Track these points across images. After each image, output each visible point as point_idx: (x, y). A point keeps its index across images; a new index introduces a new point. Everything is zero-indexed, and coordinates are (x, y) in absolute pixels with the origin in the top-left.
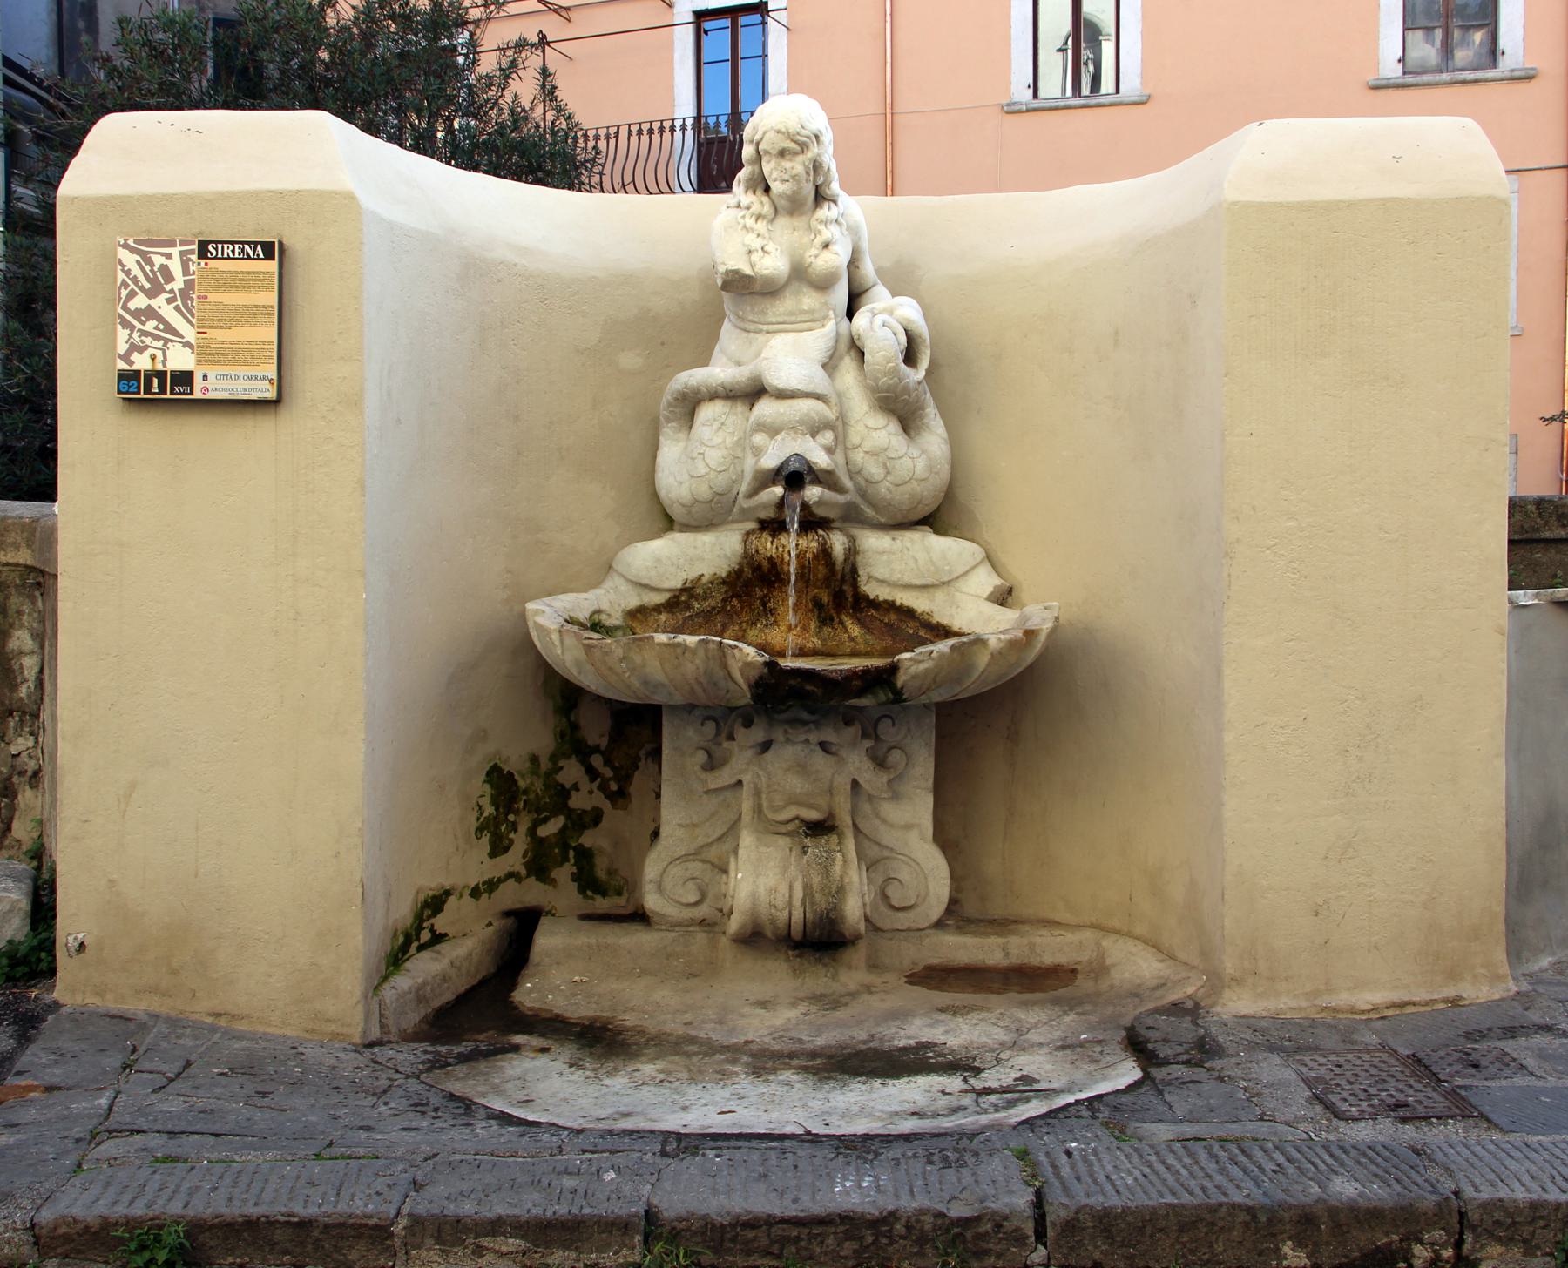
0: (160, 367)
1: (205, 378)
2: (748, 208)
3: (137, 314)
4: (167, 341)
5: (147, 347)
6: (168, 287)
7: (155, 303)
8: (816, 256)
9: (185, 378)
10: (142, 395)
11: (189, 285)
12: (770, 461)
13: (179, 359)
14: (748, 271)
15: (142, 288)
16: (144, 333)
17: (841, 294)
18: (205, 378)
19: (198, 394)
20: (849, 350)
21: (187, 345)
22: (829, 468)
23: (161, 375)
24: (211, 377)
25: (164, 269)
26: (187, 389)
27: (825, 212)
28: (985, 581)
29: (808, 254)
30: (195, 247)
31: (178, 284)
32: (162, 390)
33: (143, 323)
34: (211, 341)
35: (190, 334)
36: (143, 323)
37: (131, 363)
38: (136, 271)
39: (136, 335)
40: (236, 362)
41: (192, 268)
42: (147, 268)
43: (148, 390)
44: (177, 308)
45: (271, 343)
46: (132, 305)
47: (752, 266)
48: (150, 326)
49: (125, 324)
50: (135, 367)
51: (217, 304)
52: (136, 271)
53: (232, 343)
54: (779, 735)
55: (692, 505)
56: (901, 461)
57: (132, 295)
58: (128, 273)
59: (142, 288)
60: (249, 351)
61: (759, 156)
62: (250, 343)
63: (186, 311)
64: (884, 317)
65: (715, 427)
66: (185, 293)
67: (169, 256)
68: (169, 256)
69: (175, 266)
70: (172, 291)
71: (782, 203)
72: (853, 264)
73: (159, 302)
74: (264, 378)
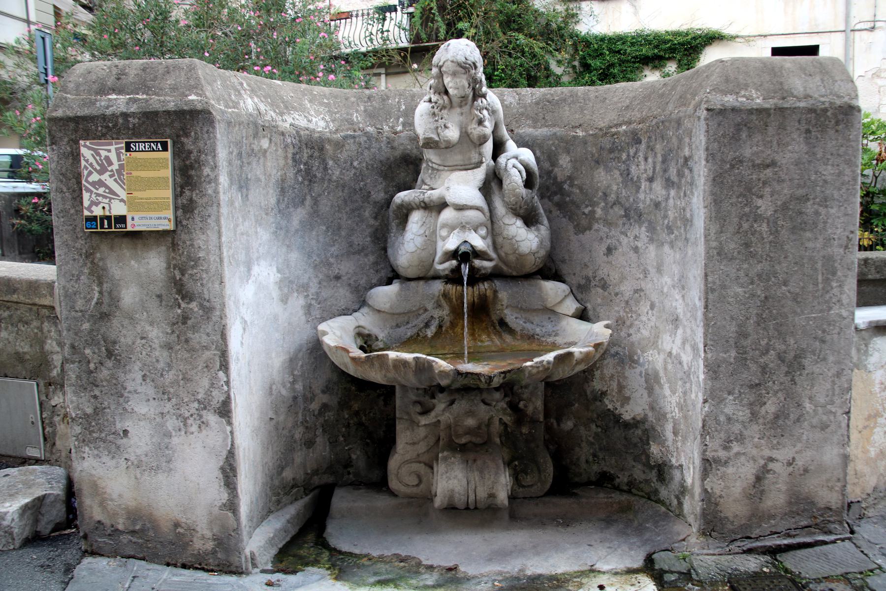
0: (108, 214)
1: (133, 219)
2: (436, 103)
3: (93, 184)
4: (111, 199)
5: (100, 203)
6: (110, 169)
7: (103, 177)
8: (475, 129)
9: (122, 219)
10: (99, 230)
11: (121, 167)
12: (452, 244)
13: (118, 209)
14: (437, 139)
15: (95, 169)
16: (98, 195)
17: (489, 147)
18: (133, 219)
19: (129, 228)
20: (494, 179)
21: (122, 200)
22: (484, 249)
23: (109, 218)
24: (136, 218)
25: (107, 159)
26: (123, 226)
27: (480, 102)
28: (571, 306)
29: (469, 128)
30: (124, 145)
31: (115, 167)
32: (110, 227)
33: (97, 189)
34: (135, 198)
35: (123, 194)
36: (97, 189)
37: (92, 212)
38: (92, 160)
39: (93, 196)
40: (150, 210)
41: (122, 157)
42: (98, 158)
43: (102, 227)
44: (115, 180)
45: (168, 198)
46: (91, 179)
47: (438, 135)
48: (101, 190)
49: (88, 190)
50: (94, 214)
51: (137, 177)
52: (92, 160)
53: (146, 199)
54: (457, 396)
55: (408, 268)
56: (524, 242)
57: (90, 173)
58: (87, 161)
59: (95, 169)
60: (156, 203)
61: (440, 75)
62: (156, 198)
63: (120, 181)
64: (514, 161)
65: (420, 224)
66: (120, 171)
67: (109, 151)
68: (109, 151)
69: (113, 156)
70: (112, 171)
71: (455, 100)
72: (494, 132)
73: (105, 177)
74: (165, 218)
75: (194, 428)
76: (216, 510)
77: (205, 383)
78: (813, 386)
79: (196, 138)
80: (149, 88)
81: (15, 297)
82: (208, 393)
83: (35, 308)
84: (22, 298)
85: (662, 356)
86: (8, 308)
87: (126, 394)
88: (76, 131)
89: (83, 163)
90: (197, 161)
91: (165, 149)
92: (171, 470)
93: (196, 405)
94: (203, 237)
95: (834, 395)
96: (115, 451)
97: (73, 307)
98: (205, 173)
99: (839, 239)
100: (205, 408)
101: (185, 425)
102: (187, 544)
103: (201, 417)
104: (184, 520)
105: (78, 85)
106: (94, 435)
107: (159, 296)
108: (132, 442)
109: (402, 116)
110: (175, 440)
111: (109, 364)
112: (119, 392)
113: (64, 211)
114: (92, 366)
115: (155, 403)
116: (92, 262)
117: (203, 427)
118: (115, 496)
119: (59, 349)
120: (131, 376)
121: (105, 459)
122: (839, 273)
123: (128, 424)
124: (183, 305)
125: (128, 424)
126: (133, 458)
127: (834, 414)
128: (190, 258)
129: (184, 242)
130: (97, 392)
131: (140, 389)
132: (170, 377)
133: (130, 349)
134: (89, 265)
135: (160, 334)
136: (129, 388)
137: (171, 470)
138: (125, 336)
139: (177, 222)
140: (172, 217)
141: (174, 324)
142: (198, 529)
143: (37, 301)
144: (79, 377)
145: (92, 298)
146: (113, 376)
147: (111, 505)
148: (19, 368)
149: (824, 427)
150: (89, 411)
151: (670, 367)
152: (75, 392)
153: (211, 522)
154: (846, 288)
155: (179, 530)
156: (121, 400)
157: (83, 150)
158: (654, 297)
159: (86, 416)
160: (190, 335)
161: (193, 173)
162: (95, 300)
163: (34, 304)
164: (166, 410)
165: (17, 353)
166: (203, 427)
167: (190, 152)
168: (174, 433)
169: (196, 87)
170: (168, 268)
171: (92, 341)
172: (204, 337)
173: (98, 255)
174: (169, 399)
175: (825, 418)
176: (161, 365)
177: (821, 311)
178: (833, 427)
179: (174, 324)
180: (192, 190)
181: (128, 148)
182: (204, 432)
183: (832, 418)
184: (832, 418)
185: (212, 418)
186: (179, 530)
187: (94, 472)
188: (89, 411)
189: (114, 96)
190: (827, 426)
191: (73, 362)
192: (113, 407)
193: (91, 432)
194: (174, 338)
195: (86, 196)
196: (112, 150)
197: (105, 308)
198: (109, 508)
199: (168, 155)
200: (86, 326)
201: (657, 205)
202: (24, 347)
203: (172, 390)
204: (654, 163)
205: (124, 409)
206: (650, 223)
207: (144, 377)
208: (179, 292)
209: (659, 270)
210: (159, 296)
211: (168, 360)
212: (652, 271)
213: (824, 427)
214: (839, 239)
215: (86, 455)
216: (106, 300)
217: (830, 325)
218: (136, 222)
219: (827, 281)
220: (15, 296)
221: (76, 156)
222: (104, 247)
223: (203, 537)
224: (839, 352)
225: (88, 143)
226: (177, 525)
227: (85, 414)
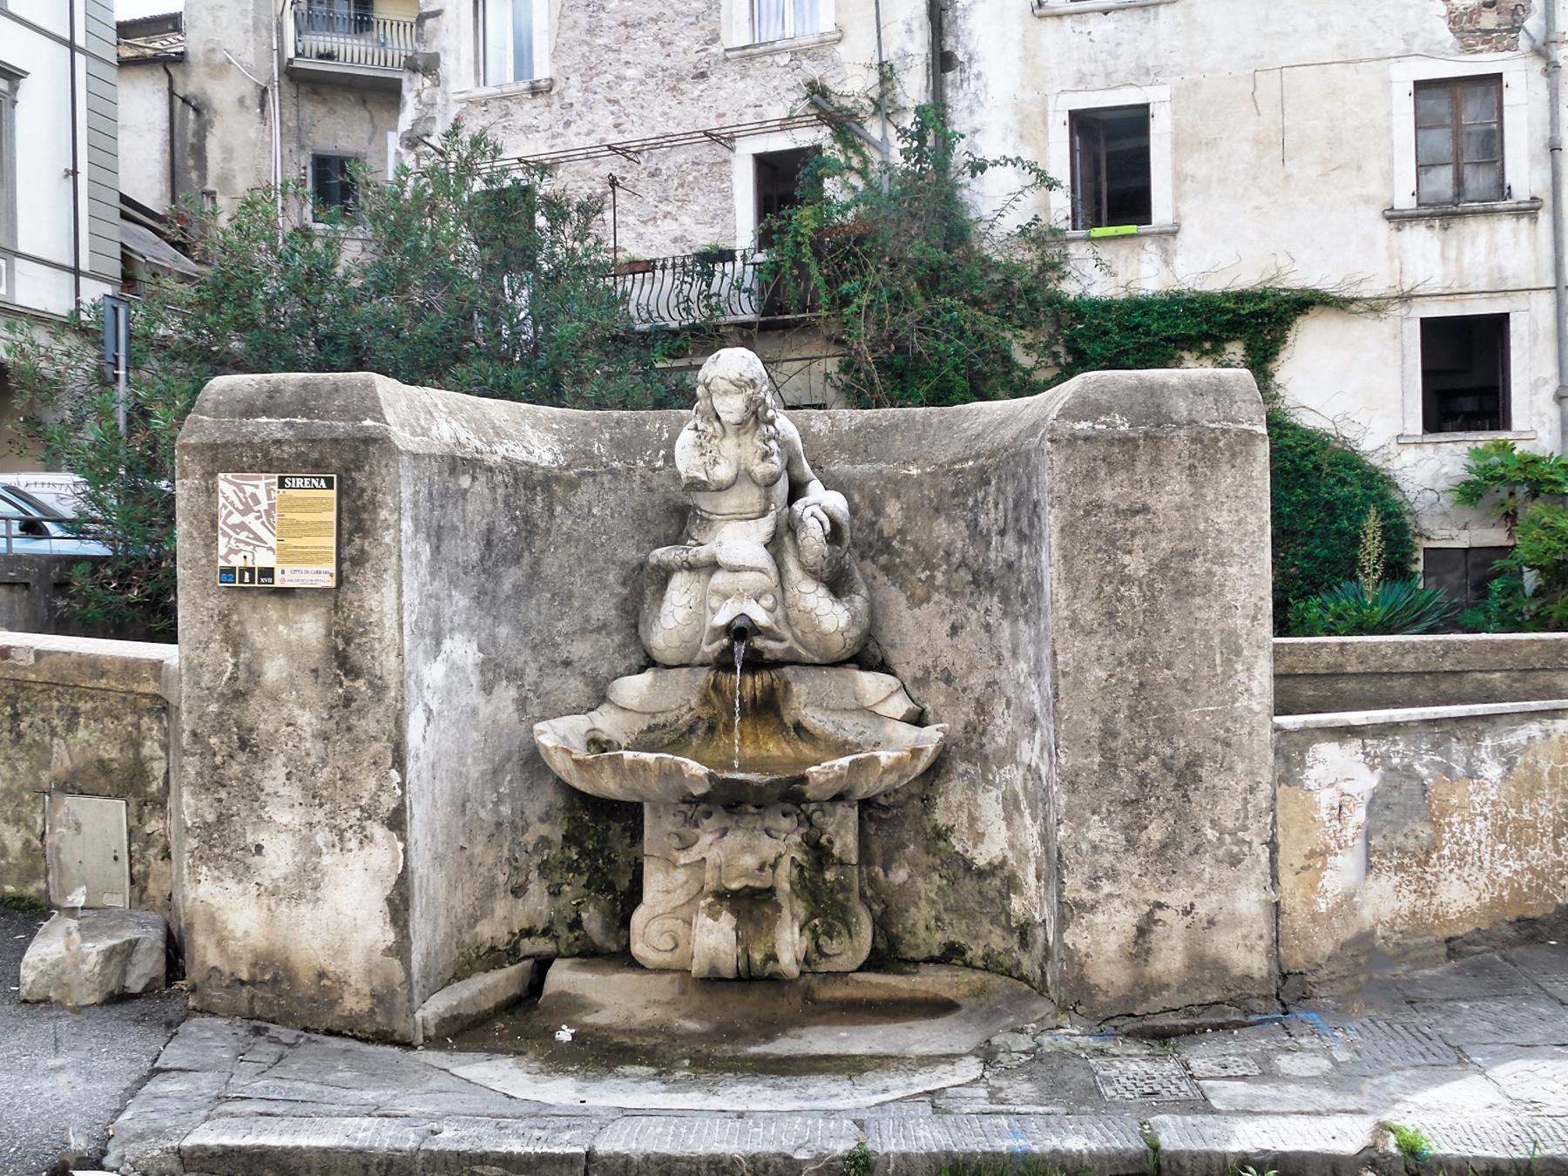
0: (250, 565)
3: (234, 527)
9: (268, 572)
11: (272, 506)
13: (264, 559)
16: (238, 541)
19: (278, 584)
21: (270, 549)
23: (251, 570)
31: (264, 506)
34: (287, 547)
35: (272, 541)
38: (233, 498)
40: (305, 561)
41: (273, 495)
46: (230, 521)
48: (243, 535)
49: (225, 534)
52: (233, 498)
57: (230, 513)
63: (268, 525)
66: (269, 513)
67: (257, 487)
68: (257, 487)
69: (261, 494)
73: (250, 519)
75: (353, 844)
76: (378, 957)
77: (372, 784)
78: (1215, 803)
79: (372, 473)
80: (311, 410)
81: (103, 683)
82: (375, 798)
83: (130, 697)
84: (113, 683)
85: (1021, 771)
86: (92, 698)
87: (263, 798)
88: (214, 460)
89: (221, 501)
90: (373, 502)
91: (330, 486)
92: (318, 899)
93: (358, 813)
94: (377, 596)
95: (1246, 817)
96: (243, 872)
97: (197, 683)
98: (382, 517)
99: (1243, 607)
100: (370, 818)
101: (341, 840)
102: (336, 1001)
103: (363, 829)
104: (331, 968)
105: (217, 404)
106: (216, 850)
107: (314, 671)
108: (267, 861)
109: (664, 447)
110: (326, 860)
111: (242, 757)
112: (253, 793)
113: (193, 561)
114: (218, 760)
115: (302, 810)
116: (227, 626)
117: (366, 842)
118: (239, 934)
119: (162, 754)
120: (272, 773)
121: (229, 883)
122: (1245, 652)
123: (263, 837)
124: (346, 683)
125: (263, 837)
126: (267, 883)
127: (1250, 844)
128: (358, 622)
129: (351, 603)
130: (223, 795)
131: (282, 791)
132: (323, 775)
133: (272, 737)
134: (222, 629)
135: (314, 720)
136: (268, 790)
137: (318, 899)
138: (265, 721)
139: (340, 578)
140: (333, 570)
141: (333, 707)
142: (352, 981)
143: (135, 686)
144: (200, 774)
145: (224, 672)
146: (246, 773)
147: (232, 946)
148: (102, 781)
149: (1235, 861)
150: (211, 818)
151: (1030, 784)
152: (193, 794)
153: (369, 972)
154: (1256, 672)
155: (325, 982)
156: (256, 805)
157: (222, 485)
158: (1010, 692)
159: (207, 825)
160: (353, 721)
161: (365, 516)
162: (228, 675)
163: (131, 692)
164: (316, 819)
165: (101, 761)
166: (366, 842)
167: (363, 490)
168: (325, 850)
169: (376, 412)
170: (328, 635)
171: (220, 727)
172: (373, 724)
173: (235, 617)
174: (321, 805)
175: (1235, 849)
176: (311, 761)
177: (1223, 703)
178: (1248, 861)
179: (333, 707)
180: (364, 538)
181: (282, 485)
182: (367, 848)
183: (1246, 849)
184: (1246, 849)
185: (378, 831)
186: (325, 982)
187: (212, 901)
188: (211, 818)
189: (264, 419)
190: (1240, 861)
191: (193, 755)
192: (243, 814)
193: (211, 847)
194: (332, 724)
195: (222, 541)
196: (261, 486)
197: (240, 685)
198: (231, 948)
199: (333, 493)
200: (213, 708)
201: (1010, 566)
202: (110, 752)
203: (325, 793)
204: (1006, 510)
205: (259, 817)
206: (1003, 590)
207: (289, 776)
208: (341, 666)
209: (1015, 654)
210: (314, 671)
211: (323, 754)
212: (1007, 654)
213: (1235, 861)
214: (1243, 607)
215: (202, 877)
216: (242, 674)
217: (1236, 721)
218: (287, 576)
219: (1228, 662)
220: (104, 681)
221: (211, 492)
222: (245, 607)
223: (357, 993)
224: (1251, 759)
225: (229, 476)
226: (322, 975)
227: (205, 823)
